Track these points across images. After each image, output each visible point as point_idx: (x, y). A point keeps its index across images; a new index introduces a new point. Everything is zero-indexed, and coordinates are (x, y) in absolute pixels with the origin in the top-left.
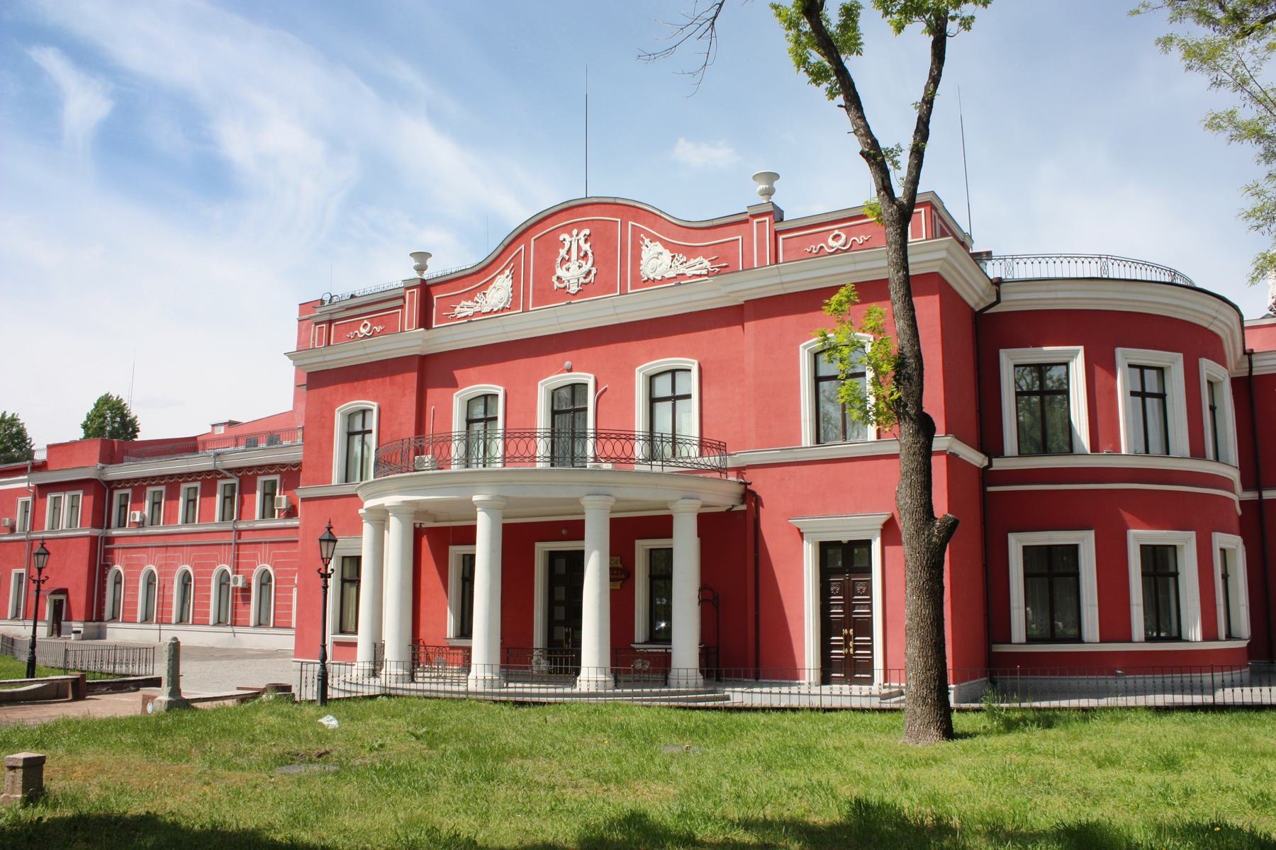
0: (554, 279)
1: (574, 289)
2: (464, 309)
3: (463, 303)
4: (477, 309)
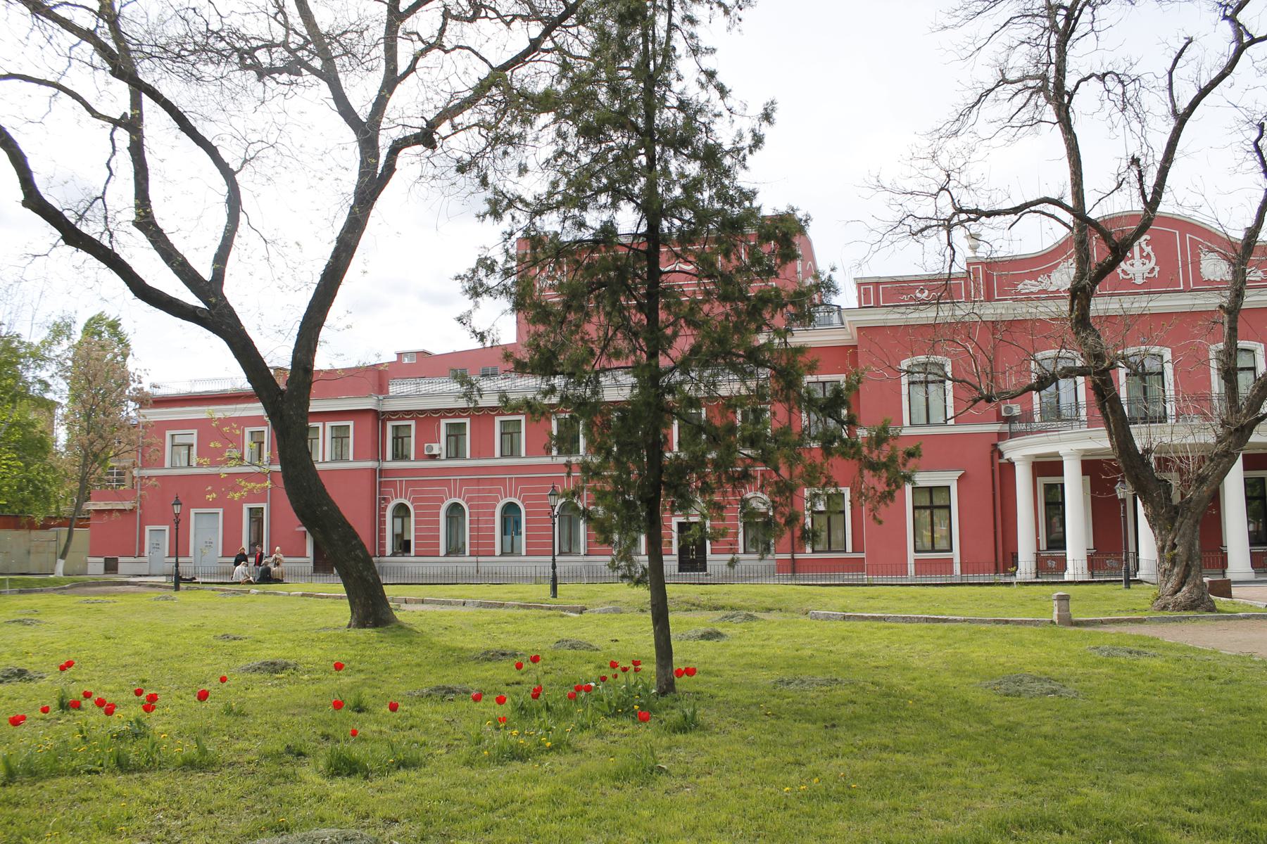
1: (1139, 281)
2: (1028, 286)
3: (1027, 281)
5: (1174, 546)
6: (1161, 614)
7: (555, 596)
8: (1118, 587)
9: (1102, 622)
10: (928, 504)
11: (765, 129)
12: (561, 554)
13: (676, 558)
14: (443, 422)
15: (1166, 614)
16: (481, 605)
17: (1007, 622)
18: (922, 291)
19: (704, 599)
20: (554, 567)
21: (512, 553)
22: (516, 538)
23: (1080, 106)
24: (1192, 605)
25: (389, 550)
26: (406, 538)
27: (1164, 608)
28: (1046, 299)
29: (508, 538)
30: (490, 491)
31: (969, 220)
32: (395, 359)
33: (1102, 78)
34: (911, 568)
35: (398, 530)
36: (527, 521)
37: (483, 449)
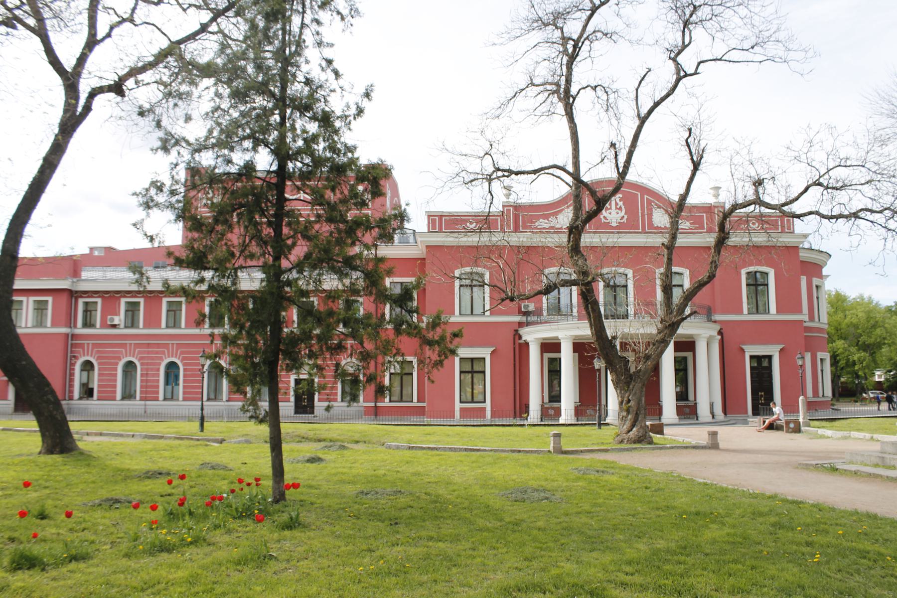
0: (602, 217)
1: (614, 224)
2: (542, 223)
4: (552, 225)
5: (629, 401)
6: (619, 446)
7: (202, 430)
8: (594, 427)
9: (582, 451)
10: (470, 369)
11: (365, 104)
12: (209, 399)
13: (293, 404)
14: (123, 301)
15: (623, 446)
16: (146, 437)
17: (519, 451)
18: (471, 223)
19: (311, 434)
20: (202, 409)
21: (172, 399)
22: (175, 388)
23: (579, 106)
24: (639, 440)
25: (76, 395)
26: (90, 386)
27: (622, 442)
28: (555, 232)
29: (169, 387)
30: (157, 353)
31: (504, 176)
32: (87, 251)
33: (595, 88)
34: (457, 414)
35: (85, 380)
36: (185, 376)
37: (152, 321)
